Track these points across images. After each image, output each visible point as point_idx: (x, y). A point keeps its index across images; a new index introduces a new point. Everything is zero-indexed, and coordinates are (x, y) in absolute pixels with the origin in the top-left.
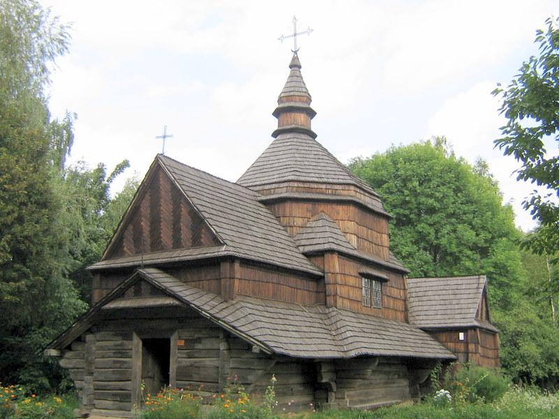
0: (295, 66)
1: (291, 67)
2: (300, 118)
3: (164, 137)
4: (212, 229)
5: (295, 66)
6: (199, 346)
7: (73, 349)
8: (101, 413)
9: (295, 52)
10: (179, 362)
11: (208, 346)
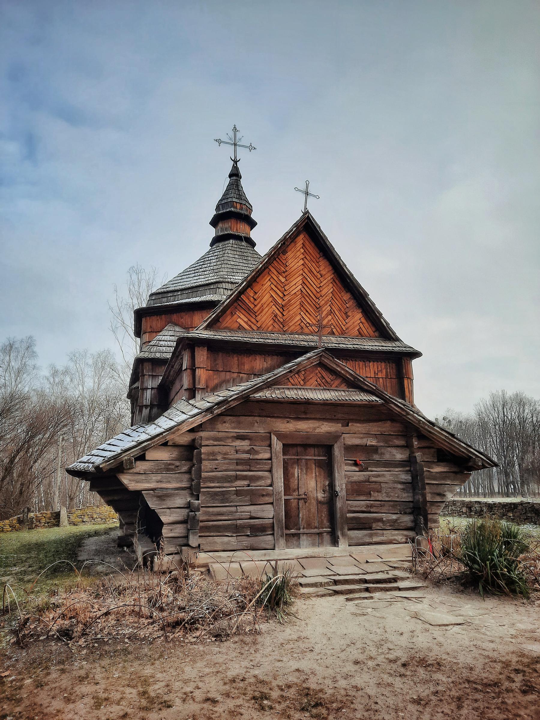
0: (235, 174)
1: (231, 176)
2: (241, 229)
3: (307, 194)
4: (382, 320)
5: (235, 174)
6: (376, 457)
7: (147, 458)
8: (220, 557)
9: (236, 162)
10: (349, 477)
11: (387, 457)
